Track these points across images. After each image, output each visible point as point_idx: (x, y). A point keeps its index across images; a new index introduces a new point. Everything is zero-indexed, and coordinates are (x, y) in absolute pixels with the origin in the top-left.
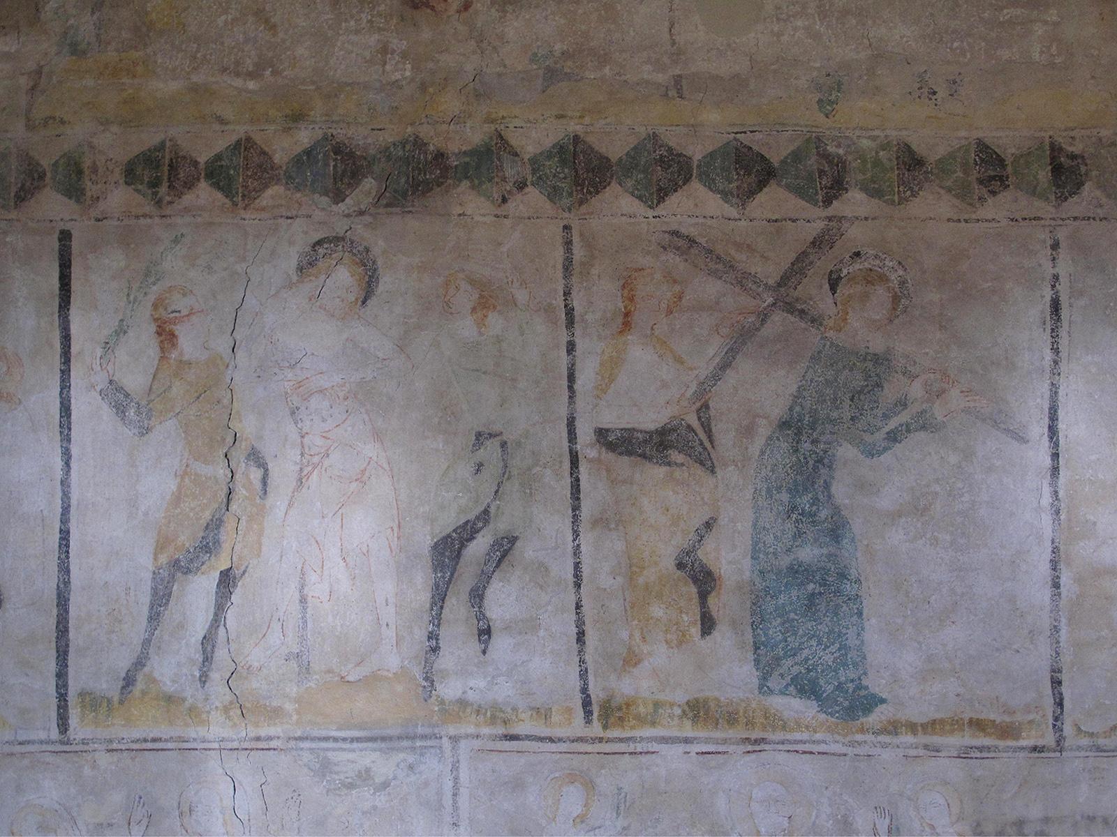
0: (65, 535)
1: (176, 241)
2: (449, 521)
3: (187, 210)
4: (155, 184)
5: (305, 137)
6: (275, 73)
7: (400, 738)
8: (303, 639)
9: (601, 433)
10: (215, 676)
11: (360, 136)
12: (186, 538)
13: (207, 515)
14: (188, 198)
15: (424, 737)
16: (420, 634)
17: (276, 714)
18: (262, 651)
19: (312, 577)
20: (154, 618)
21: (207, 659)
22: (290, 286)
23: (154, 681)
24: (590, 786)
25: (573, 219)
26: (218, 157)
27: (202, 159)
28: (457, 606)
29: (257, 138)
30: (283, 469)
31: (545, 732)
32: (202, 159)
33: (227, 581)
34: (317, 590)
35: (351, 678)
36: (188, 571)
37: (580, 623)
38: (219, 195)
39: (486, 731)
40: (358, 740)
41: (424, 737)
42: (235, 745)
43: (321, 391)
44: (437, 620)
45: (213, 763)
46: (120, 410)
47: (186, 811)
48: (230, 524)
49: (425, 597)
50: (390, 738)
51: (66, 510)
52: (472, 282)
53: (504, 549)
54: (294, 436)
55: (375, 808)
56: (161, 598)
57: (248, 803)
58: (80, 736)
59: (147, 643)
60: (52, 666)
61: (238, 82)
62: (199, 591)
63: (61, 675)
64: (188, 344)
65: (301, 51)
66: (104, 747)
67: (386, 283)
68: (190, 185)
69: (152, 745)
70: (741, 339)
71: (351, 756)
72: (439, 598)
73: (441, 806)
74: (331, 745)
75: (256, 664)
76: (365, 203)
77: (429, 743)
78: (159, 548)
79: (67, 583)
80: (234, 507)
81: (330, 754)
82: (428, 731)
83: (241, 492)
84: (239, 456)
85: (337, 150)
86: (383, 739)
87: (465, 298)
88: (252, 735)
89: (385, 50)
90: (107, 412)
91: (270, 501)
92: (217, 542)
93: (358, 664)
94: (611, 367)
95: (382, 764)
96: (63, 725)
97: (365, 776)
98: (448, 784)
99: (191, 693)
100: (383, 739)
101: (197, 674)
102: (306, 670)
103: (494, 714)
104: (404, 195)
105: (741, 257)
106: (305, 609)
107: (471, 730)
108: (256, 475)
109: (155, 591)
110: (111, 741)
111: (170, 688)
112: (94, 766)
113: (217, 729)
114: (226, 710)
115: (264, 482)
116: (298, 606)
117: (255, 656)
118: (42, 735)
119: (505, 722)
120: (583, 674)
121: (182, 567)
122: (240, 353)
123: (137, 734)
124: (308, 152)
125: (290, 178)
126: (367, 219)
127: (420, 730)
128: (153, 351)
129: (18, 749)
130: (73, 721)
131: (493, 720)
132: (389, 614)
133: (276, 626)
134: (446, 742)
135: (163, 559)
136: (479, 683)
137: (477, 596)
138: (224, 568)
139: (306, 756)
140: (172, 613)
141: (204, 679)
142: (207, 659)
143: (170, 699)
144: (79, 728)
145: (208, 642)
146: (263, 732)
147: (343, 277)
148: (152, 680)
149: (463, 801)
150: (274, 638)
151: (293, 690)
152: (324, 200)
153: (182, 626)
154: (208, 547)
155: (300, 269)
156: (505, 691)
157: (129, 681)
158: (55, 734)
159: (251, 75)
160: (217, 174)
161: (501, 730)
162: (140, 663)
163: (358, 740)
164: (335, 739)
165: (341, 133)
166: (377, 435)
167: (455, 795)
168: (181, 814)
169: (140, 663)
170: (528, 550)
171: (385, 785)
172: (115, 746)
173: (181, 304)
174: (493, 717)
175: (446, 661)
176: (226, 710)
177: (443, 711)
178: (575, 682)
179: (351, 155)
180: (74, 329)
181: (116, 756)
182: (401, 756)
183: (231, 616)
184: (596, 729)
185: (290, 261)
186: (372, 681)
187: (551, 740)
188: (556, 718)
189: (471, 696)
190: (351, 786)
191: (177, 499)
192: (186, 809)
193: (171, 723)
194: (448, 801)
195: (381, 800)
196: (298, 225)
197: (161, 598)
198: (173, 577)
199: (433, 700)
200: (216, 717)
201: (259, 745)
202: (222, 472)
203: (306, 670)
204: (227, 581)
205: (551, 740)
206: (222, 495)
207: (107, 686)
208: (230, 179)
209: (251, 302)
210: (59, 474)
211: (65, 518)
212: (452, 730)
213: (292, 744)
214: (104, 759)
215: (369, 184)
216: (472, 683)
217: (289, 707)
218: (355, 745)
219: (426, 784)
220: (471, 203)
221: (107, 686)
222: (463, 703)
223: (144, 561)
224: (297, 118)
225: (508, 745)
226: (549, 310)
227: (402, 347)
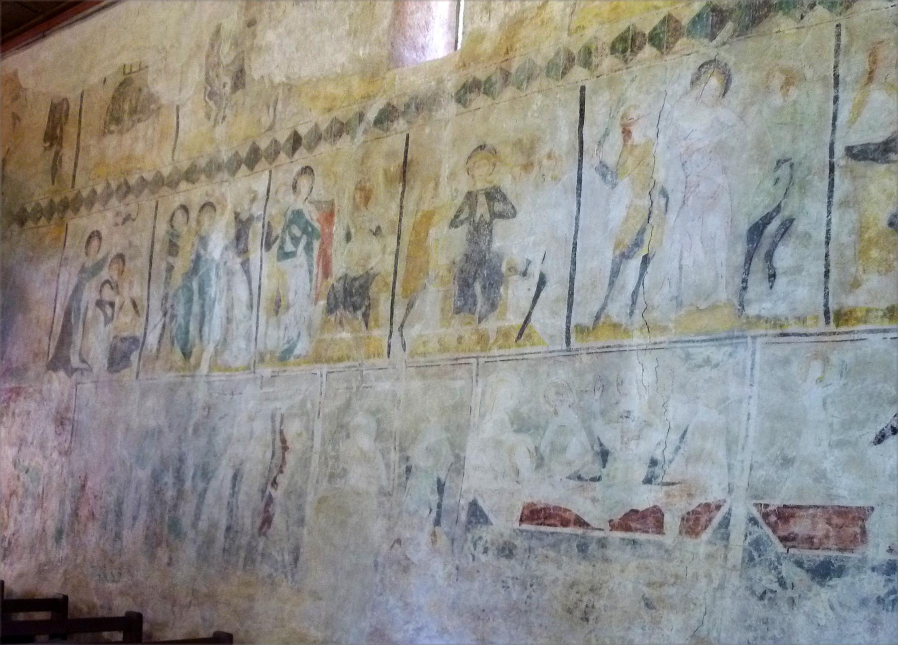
0: (575, 245)
2: (758, 214)
7: (726, 338)
8: (679, 288)
10: (637, 312)
12: (628, 240)
15: (738, 337)
16: (738, 280)
17: (664, 329)
18: (659, 297)
19: (686, 254)
20: (612, 284)
21: (634, 303)
24: (826, 361)
30: (675, 198)
31: (802, 330)
33: (646, 260)
34: (688, 261)
35: (701, 308)
37: (827, 266)
39: (771, 332)
40: (704, 341)
41: (738, 337)
42: (644, 347)
45: (634, 357)
47: (620, 383)
48: (648, 232)
50: (721, 339)
55: (710, 377)
56: (615, 273)
57: (648, 378)
59: (607, 297)
63: (569, 317)
66: (585, 352)
71: (701, 350)
73: (744, 375)
74: (691, 344)
75: (656, 304)
77: (740, 340)
78: (617, 246)
79: (574, 270)
81: (690, 350)
82: (740, 334)
86: (717, 340)
88: (653, 341)
91: (668, 216)
92: (642, 241)
93: (706, 299)
95: (717, 353)
96: (568, 342)
97: (707, 361)
98: (749, 363)
99: (624, 320)
100: (717, 340)
101: (628, 311)
102: (680, 305)
103: (776, 322)
107: (763, 332)
109: (612, 269)
110: (588, 349)
111: (615, 319)
112: (581, 362)
113: (637, 339)
114: (641, 329)
116: (678, 271)
117: (657, 299)
118: (559, 348)
119: (781, 326)
120: (826, 296)
121: (625, 256)
123: (600, 344)
127: (736, 334)
130: (572, 340)
131: (775, 326)
132: (723, 271)
133: (667, 282)
134: (749, 340)
135: (618, 252)
136: (767, 305)
138: (644, 254)
139: (679, 351)
140: (619, 281)
142: (634, 303)
143: (616, 326)
144: (574, 344)
145: (635, 294)
146: (659, 339)
148: (608, 316)
149: (757, 373)
150: (666, 289)
151: (673, 316)
153: (623, 287)
156: (782, 309)
157: (598, 317)
158: (564, 347)
161: (779, 331)
163: (704, 341)
164: (693, 342)
167: (752, 369)
168: (618, 385)
169: (603, 308)
171: (717, 365)
172: (590, 351)
174: (775, 324)
175: (750, 294)
176: (641, 329)
177: (749, 322)
178: (821, 299)
182: (726, 348)
183: (647, 280)
184: (832, 327)
186: (714, 307)
187: (806, 335)
188: (809, 322)
189: (763, 313)
190: (700, 366)
192: (620, 381)
193: (616, 338)
194: (748, 373)
195: (714, 373)
197: (615, 273)
198: (621, 262)
199: (743, 317)
200: (637, 333)
201: (655, 347)
203: (680, 305)
204: (646, 260)
205: (806, 335)
207: (587, 321)
211: (575, 237)
212: (753, 332)
213: (672, 345)
214: (585, 358)
216: (764, 305)
217: (671, 325)
218: (703, 344)
219: (738, 364)
221: (587, 321)
222: (759, 317)
223: (609, 255)
225: (782, 339)
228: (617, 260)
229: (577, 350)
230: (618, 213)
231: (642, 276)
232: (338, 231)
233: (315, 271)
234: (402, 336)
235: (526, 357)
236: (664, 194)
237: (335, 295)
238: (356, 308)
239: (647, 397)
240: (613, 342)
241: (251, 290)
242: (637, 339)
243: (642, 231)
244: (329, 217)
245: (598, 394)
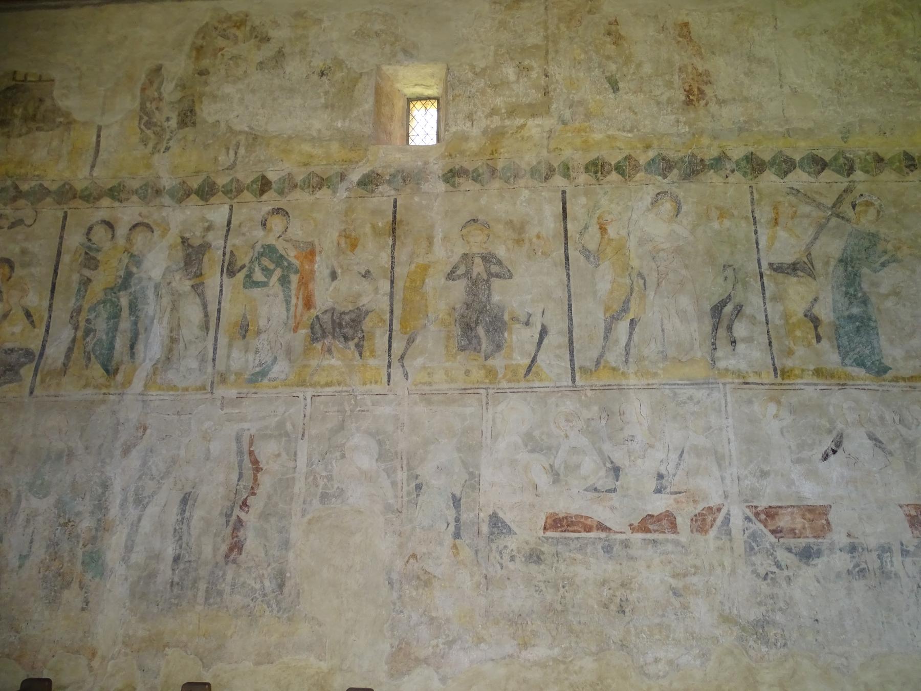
1: (605, 194)
3: (608, 182)
4: (596, 172)
5: (651, 154)
6: (638, 130)
9: (771, 265)
11: (672, 155)
12: (616, 307)
13: (623, 298)
14: (609, 178)
20: (606, 338)
21: (627, 354)
22: (649, 210)
23: (608, 362)
25: (752, 183)
26: (619, 162)
27: (613, 163)
28: (722, 332)
29: (633, 155)
32: (613, 163)
33: (633, 322)
36: (618, 319)
38: (620, 176)
43: (663, 250)
44: (715, 337)
46: (587, 258)
49: (708, 328)
51: (570, 296)
52: (717, 208)
53: (739, 310)
54: (654, 267)
56: (608, 330)
58: (580, 384)
59: (604, 347)
60: (568, 357)
61: (625, 134)
62: (622, 327)
64: (612, 232)
65: (647, 122)
67: (684, 208)
68: (609, 173)
69: (607, 388)
70: (821, 228)
72: (715, 329)
76: (675, 179)
78: (606, 311)
79: (572, 324)
80: (634, 294)
83: (636, 289)
84: (634, 274)
85: (663, 159)
87: (715, 214)
89: (678, 121)
90: (582, 258)
92: (628, 308)
94: (773, 239)
96: (574, 380)
104: (689, 175)
105: (817, 197)
106: (664, 334)
108: (641, 282)
111: (614, 365)
113: (632, 381)
115: (645, 284)
122: (631, 236)
123: (601, 383)
124: (653, 160)
125: (646, 170)
126: (676, 184)
128: (598, 235)
129: (556, 389)
130: (577, 378)
135: (608, 315)
137: (730, 328)
141: (627, 361)
142: (627, 354)
143: (614, 369)
144: (579, 382)
145: (627, 346)
147: (667, 206)
148: (607, 362)
152: (660, 178)
153: (617, 341)
154: (625, 309)
155: (652, 204)
157: (598, 363)
158: (570, 383)
159: (629, 131)
160: (619, 168)
162: (602, 355)
165: (664, 153)
166: (686, 267)
169: (602, 355)
170: (747, 310)
173: (609, 218)
179: (669, 160)
180: (569, 226)
181: (594, 392)
185: (648, 200)
191: (612, 292)
196: (650, 187)
197: (608, 330)
202: (628, 281)
206: (629, 290)
207: (590, 364)
208: (624, 170)
209: (634, 217)
210: (566, 283)
214: (589, 393)
215: (675, 171)
220: (712, 177)
221: (590, 364)
223: (600, 316)
224: (648, 147)
226: (746, 218)
227: (692, 232)
228: (609, 320)
229: (582, 386)
230: (604, 287)
231: (631, 334)
232: (321, 267)
233: (294, 301)
234: (403, 366)
235: (535, 390)
236: (640, 275)
237: (321, 326)
238: (346, 338)
239: (646, 425)
240: (612, 382)
241: (206, 315)
242: (632, 381)
243: (627, 301)
244: (311, 254)
245: (603, 422)
